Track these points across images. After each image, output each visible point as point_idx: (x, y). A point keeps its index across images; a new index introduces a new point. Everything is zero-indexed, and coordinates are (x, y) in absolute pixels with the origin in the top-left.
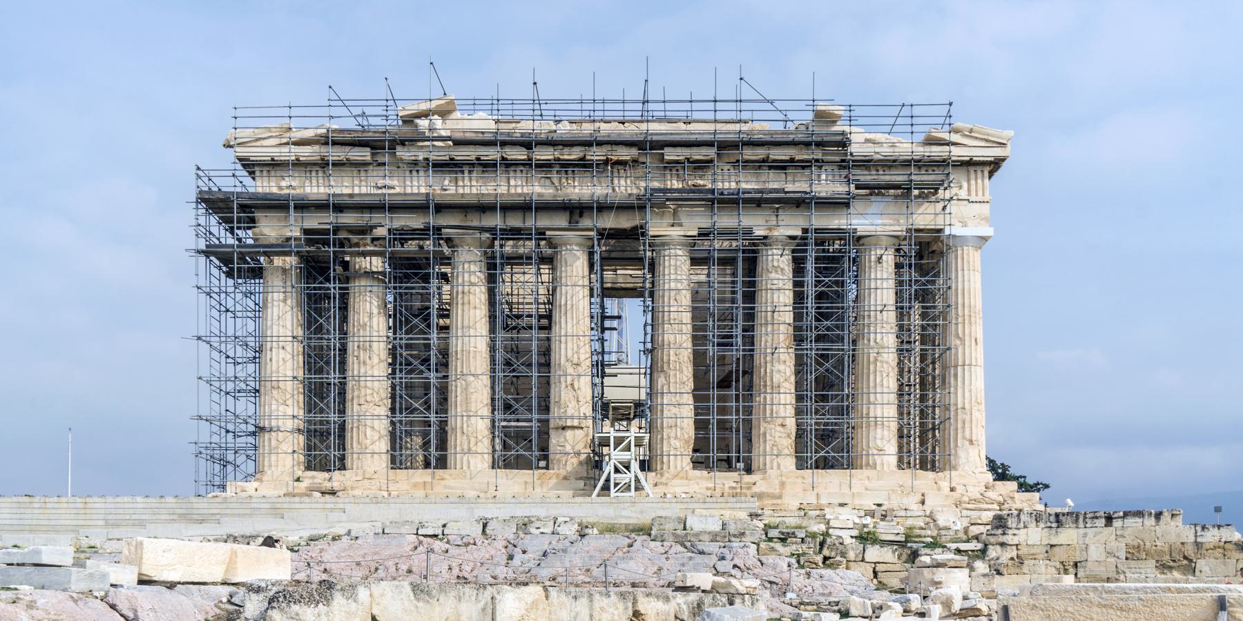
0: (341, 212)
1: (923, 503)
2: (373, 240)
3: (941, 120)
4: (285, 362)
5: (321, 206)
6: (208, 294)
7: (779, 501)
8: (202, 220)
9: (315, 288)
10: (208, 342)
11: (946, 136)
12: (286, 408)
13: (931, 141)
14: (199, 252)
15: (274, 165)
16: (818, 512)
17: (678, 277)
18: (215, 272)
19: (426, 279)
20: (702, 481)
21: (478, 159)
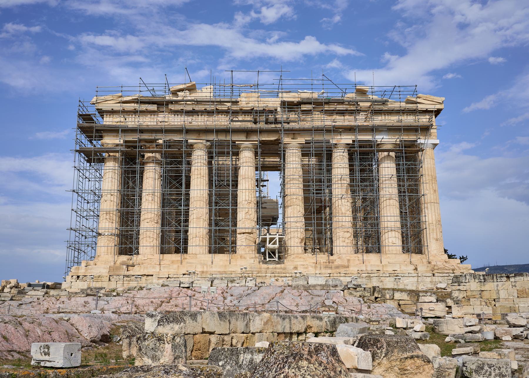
0: (142, 133)
1: (416, 269)
2: (157, 145)
3: (412, 93)
4: (110, 203)
5: (133, 131)
6: (79, 170)
7: (348, 269)
8: (78, 137)
9: (128, 168)
10: (77, 193)
11: (414, 99)
12: (109, 224)
13: (409, 102)
14: (77, 151)
15: (113, 112)
16: (367, 275)
17: (294, 161)
18: (82, 160)
19: (180, 163)
20: (310, 258)
21: (205, 110)
